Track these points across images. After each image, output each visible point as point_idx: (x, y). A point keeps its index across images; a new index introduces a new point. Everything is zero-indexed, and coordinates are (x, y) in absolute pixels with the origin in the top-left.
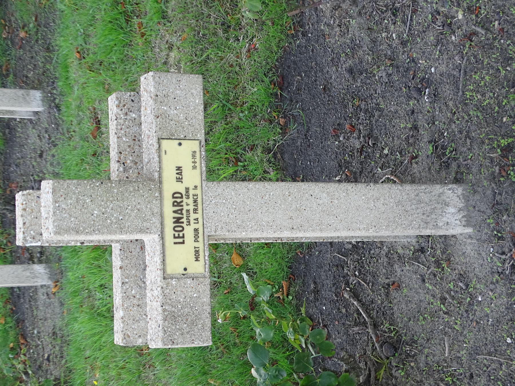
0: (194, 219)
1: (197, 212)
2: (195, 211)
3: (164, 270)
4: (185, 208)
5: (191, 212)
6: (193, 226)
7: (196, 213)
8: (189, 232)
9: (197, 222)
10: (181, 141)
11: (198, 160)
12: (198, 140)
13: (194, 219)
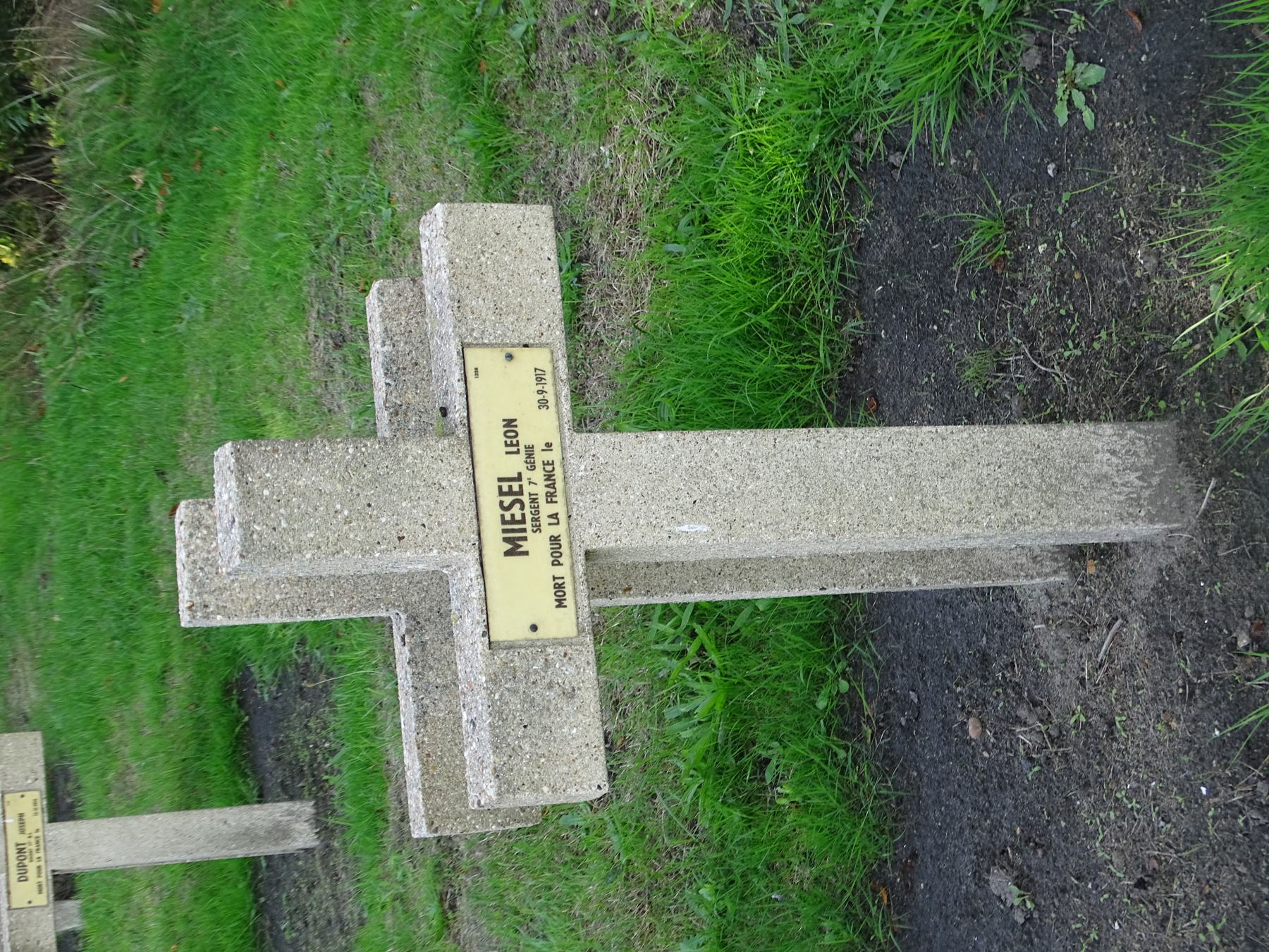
0: (550, 516)
2: (550, 497)
3: (487, 633)
4: (527, 489)
5: (542, 500)
6: (548, 531)
7: (552, 502)
10: (509, 350)
11: (549, 388)
13: (550, 516)
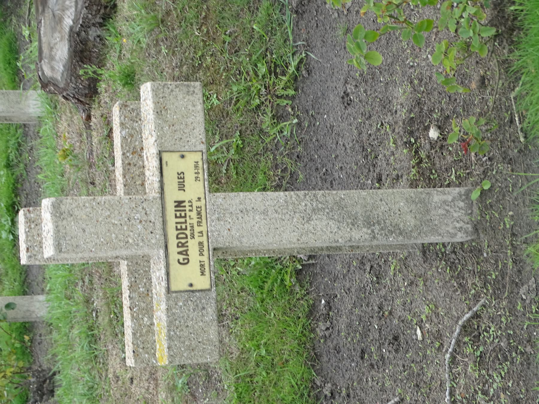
0: (199, 233)
1: (201, 224)
2: (199, 224)
6: (197, 239)
8: (193, 246)
9: (201, 235)
12: (200, 151)
13: (199, 233)
